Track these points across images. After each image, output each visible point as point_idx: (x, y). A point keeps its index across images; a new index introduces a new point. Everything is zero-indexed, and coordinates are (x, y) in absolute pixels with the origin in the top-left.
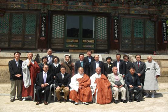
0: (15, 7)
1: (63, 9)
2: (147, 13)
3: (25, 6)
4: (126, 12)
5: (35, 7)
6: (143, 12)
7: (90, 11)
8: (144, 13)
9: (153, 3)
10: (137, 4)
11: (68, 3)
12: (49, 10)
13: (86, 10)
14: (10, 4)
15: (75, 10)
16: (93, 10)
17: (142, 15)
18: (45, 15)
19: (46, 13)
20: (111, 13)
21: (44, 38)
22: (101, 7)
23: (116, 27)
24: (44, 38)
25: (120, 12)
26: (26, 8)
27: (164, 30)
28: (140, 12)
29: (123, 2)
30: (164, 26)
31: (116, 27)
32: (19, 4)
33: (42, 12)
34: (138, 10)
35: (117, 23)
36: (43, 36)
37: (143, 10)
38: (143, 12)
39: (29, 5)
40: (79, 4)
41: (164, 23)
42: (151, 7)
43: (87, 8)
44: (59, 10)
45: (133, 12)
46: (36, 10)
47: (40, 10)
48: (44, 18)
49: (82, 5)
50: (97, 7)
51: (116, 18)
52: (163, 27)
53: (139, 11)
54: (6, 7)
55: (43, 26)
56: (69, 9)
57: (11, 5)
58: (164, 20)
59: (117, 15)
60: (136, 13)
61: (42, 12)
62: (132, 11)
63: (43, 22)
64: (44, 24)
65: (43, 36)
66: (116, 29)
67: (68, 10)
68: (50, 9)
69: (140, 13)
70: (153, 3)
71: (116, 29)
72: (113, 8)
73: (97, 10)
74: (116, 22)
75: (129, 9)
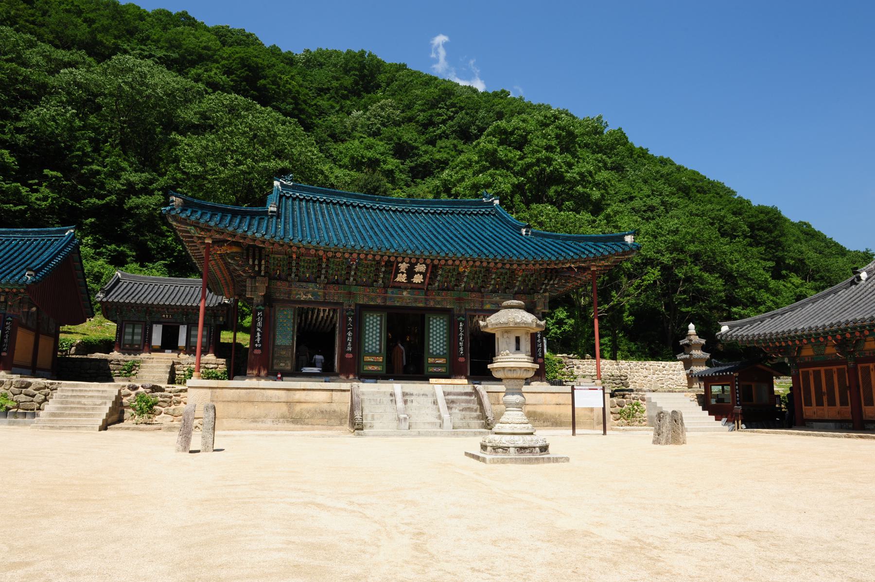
0: (303, 297)
1: (379, 301)
4: (477, 306)
7: (421, 305)
11: (386, 292)
12: (356, 305)
13: (414, 305)
14: (294, 292)
19: (352, 310)
21: (351, 356)
22: (439, 298)
23: (461, 334)
24: (351, 356)
26: (321, 299)
31: (461, 334)
32: (308, 292)
33: (346, 307)
35: (463, 327)
36: (349, 352)
39: (325, 294)
40: (405, 293)
43: (416, 300)
46: (337, 303)
47: (342, 304)
51: (461, 318)
55: (349, 334)
56: (388, 303)
57: (297, 294)
59: (463, 312)
61: (346, 307)
65: (349, 352)
68: (358, 302)
72: (456, 299)
73: (432, 304)
75: (482, 302)
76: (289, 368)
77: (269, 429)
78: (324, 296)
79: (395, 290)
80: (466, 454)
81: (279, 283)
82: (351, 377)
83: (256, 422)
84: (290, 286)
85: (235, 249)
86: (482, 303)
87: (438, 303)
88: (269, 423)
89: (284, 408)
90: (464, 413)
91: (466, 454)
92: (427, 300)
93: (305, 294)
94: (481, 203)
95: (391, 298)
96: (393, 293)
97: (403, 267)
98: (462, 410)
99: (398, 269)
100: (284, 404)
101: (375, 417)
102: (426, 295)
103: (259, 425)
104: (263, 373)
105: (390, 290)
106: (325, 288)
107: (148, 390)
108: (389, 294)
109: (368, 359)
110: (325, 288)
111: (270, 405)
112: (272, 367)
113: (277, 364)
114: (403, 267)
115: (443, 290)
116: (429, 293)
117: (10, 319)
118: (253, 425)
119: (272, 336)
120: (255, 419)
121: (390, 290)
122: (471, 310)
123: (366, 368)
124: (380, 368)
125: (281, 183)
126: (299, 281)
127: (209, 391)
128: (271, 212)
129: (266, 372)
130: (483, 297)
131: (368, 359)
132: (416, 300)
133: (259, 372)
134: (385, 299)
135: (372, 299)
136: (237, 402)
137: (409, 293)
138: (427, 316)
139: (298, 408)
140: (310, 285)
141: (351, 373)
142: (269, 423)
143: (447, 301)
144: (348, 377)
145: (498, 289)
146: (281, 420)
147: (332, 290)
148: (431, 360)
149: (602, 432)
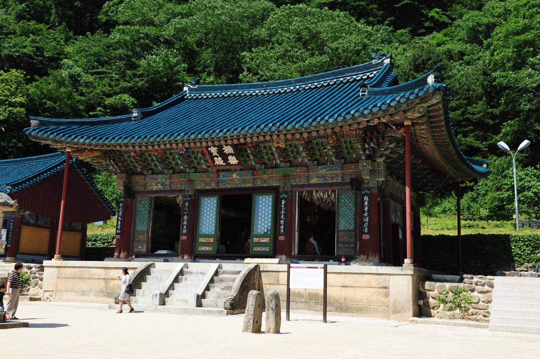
0: (155, 188)
1: (213, 186)
2: (339, 180)
3: (166, 185)
4: (303, 182)
5: (179, 186)
6: (332, 179)
7: (249, 185)
8: (334, 181)
9: (354, 157)
10: (324, 164)
11: (218, 176)
12: (196, 190)
13: (243, 186)
14: (148, 184)
15: (229, 187)
16: (253, 183)
17: (331, 185)
18: (189, 199)
20: (279, 186)
22: (265, 177)
23: (283, 212)
25: (293, 183)
26: (168, 188)
27: (364, 212)
28: (327, 178)
29: (300, 163)
30: (366, 203)
31: (283, 212)
32: (158, 183)
34: (323, 177)
36: (184, 234)
37: (333, 174)
38: (332, 179)
39: (171, 183)
40: (234, 175)
41: (365, 198)
42: (345, 165)
43: (244, 181)
44: (207, 188)
45: (314, 181)
47: (184, 191)
48: (187, 204)
49: (238, 177)
50: (259, 178)
52: (364, 206)
53: (325, 178)
54: (145, 189)
56: (221, 186)
57: (151, 185)
58: (366, 191)
60: (320, 181)
62: (313, 178)
63: (186, 211)
64: (187, 215)
65: (184, 234)
66: (282, 216)
67: (220, 187)
69: (328, 182)
70: (354, 157)
71: (282, 216)
73: (259, 184)
74: (283, 203)
76: (144, 250)
77: (91, 302)
78: (170, 185)
79: (226, 173)
80: (66, 325)
81: (138, 177)
82: (186, 257)
83: (84, 295)
84: (145, 179)
85: (96, 154)
86: (308, 177)
87: (265, 181)
88: (91, 297)
89: (102, 284)
90: (225, 291)
91: (66, 325)
92: (254, 180)
93: (157, 184)
94: (371, 66)
95: (223, 181)
96: (224, 176)
97: (214, 150)
98: (224, 289)
99: (210, 154)
100: (102, 281)
101: (145, 293)
102: (253, 175)
103: (86, 298)
104: (122, 255)
105: (221, 174)
106: (170, 178)
107: (38, 269)
108: (221, 178)
109: (201, 240)
110: (170, 178)
111: (93, 281)
112: (133, 250)
113: (137, 247)
114: (214, 150)
115: (273, 168)
116: (256, 172)
117: (12, 220)
118: (82, 298)
119: (133, 223)
120: (83, 293)
121: (221, 174)
122: (297, 186)
123: (200, 249)
124: (211, 249)
125: (189, 88)
126: (153, 174)
127: (56, 269)
128: (135, 117)
129: (125, 254)
130: (308, 171)
131: (201, 240)
132: (244, 181)
133: (120, 253)
134: (218, 182)
135: (207, 184)
136: (73, 278)
137: (238, 175)
138: (253, 195)
139: (112, 284)
140: (160, 176)
141: (186, 253)
142: (91, 297)
143: (273, 179)
144: (183, 257)
145: (327, 161)
146: (100, 294)
147: (176, 179)
148: (256, 240)
149: (322, 317)
